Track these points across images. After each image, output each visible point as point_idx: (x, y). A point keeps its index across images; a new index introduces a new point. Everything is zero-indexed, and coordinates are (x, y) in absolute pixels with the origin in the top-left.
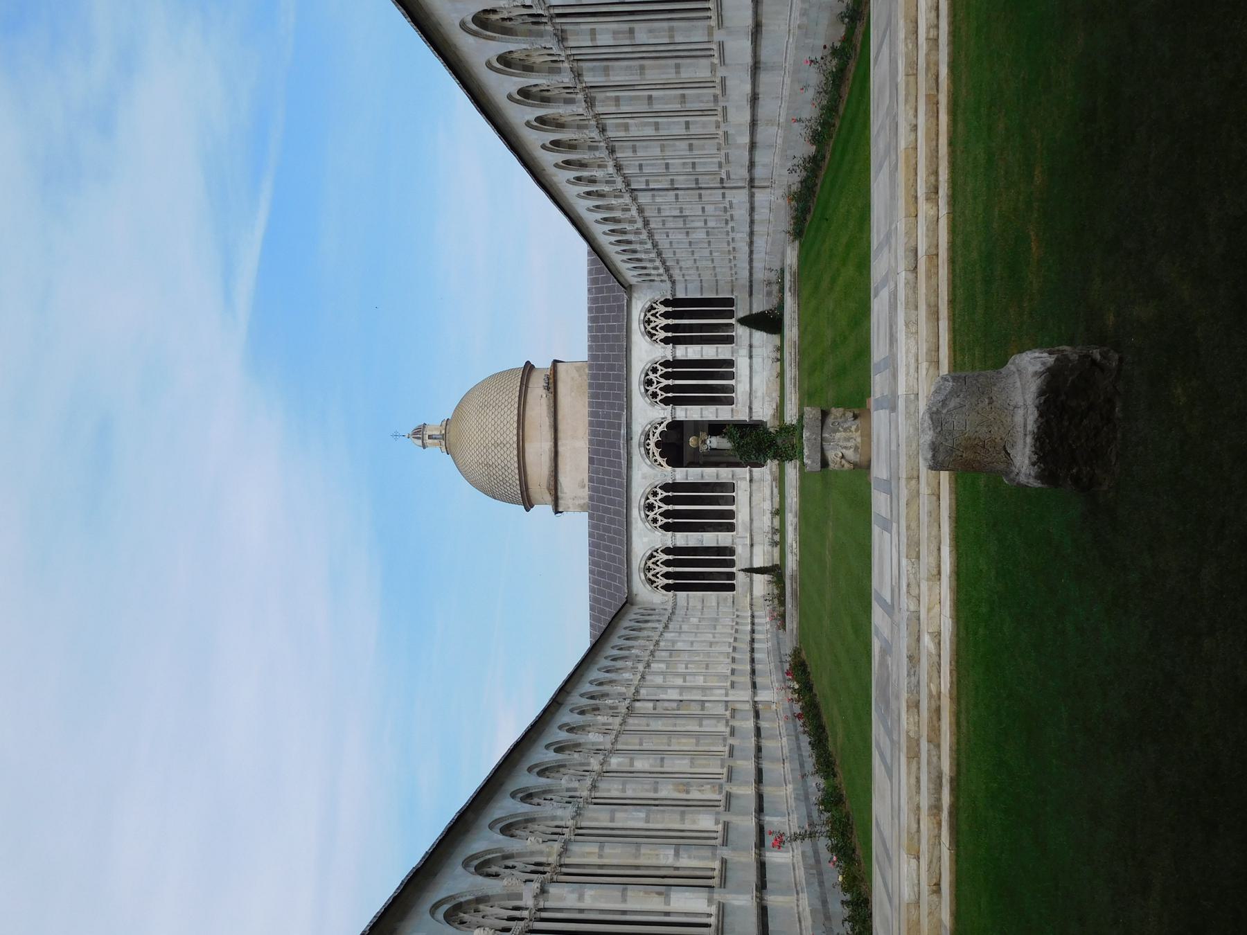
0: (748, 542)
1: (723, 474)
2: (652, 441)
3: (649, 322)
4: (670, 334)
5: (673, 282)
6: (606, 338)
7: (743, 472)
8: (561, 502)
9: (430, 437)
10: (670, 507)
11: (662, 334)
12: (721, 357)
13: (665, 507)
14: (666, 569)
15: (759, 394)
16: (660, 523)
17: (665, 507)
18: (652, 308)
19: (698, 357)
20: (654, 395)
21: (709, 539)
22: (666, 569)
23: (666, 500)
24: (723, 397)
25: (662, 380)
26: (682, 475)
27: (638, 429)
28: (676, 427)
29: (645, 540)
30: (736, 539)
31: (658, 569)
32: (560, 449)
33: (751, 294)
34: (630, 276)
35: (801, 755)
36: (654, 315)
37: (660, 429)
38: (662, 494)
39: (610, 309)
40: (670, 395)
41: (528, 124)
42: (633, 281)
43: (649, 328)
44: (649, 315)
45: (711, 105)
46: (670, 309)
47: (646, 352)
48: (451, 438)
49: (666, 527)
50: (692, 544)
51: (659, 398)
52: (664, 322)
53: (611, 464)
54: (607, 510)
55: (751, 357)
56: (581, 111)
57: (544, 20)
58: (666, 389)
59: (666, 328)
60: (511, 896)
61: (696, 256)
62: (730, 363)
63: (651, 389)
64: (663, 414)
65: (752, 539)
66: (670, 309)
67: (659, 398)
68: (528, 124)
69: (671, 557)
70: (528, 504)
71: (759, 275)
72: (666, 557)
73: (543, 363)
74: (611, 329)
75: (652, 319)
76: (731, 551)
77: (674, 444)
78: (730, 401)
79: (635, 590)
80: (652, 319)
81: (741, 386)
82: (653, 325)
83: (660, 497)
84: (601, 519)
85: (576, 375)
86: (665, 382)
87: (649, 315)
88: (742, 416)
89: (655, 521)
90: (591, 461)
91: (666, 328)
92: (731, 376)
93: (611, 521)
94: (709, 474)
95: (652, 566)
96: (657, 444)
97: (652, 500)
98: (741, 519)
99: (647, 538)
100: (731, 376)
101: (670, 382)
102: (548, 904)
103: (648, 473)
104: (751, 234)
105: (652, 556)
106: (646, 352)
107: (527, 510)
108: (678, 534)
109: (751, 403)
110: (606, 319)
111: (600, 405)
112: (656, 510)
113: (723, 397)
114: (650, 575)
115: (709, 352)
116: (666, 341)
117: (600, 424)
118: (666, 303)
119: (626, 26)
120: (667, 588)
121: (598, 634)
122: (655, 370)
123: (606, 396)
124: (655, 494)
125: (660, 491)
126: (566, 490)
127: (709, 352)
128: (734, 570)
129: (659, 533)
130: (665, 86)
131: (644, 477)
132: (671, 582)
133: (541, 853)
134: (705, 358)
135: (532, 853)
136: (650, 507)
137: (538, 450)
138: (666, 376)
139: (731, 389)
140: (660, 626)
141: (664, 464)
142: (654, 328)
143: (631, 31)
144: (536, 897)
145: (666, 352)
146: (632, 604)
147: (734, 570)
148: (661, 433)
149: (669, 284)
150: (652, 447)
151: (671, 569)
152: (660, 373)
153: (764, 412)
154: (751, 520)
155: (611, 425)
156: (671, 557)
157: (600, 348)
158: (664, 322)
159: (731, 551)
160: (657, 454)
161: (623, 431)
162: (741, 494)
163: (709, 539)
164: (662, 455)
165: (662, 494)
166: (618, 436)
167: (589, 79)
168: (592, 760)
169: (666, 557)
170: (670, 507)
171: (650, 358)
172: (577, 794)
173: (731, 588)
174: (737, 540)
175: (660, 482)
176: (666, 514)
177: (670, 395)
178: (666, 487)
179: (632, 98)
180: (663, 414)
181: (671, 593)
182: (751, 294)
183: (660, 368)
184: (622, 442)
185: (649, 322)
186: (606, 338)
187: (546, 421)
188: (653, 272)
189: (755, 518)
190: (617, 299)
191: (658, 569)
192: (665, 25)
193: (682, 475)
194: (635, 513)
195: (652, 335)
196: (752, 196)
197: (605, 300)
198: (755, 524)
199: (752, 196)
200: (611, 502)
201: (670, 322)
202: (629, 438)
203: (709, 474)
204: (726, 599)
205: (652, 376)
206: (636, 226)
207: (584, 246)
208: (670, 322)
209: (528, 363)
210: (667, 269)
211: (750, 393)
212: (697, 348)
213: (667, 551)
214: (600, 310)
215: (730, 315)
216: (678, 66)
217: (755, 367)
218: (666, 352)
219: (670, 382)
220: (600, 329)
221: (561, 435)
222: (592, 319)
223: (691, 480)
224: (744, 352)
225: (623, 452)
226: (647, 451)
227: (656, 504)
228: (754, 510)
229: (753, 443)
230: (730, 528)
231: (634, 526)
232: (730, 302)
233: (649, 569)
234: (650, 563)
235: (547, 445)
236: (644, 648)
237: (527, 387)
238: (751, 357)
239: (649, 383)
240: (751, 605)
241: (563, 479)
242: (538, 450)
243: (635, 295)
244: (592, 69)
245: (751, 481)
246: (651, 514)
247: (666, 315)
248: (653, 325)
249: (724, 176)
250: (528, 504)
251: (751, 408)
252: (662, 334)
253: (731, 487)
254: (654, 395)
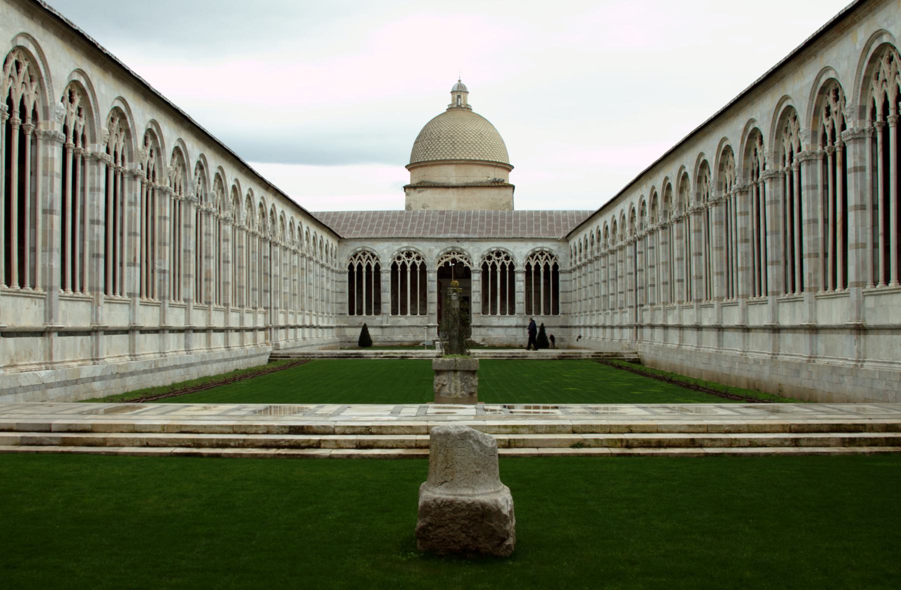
0: (384, 324)
1: (433, 308)
2: (457, 257)
3: (542, 254)
4: (533, 269)
5: (570, 272)
6: (530, 223)
7: (434, 322)
8: (412, 191)
9: (459, 97)
10: (409, 269)
11: (533, 264)
12: (517, 306)
13: (409, 266)
14: (364, 266)
15: (490, 333)
16: (397, 262)
17: (409, 266)
18: (552, 256)
19: (517, 289)
20: (489, 258)
21: (386, 297)
22: (364, 266)
23: (414, 266)
24: (488, 306)
25: (500, 263)
26: (432, 277)
27: (465, 246)
28: (465, 273)
29: (385, 251)
30: (386, 317)
31: (364, 260)
32: (450, 191)
33: (562, 327)
34: (575, 241)
35: (233, 359)
36: (547, 258)
37: (465, 262)
38: (418, 263)
39: (551, 227)
40: (490, 269)
41: (683, 167)
42: (571, 243)
43: (537, 254)
44: (547, 254)
45: (694, 297)
46: (551, 269)
47: (520, 253)
48: (459, 114)
49: (394, 266)
50: (383, 284)
51: (488, 262)
52: (542, 265)
53: (440, 227)
54: (406, 224)
55: (517, 327)
56: (692, 205)
57: (755, 179)
58: (494, 266)
59: (537, 267)
60: (130, 153)
61: (589, 288)
62: (512, 312)
63: (494, 256)
64: (476, 264)
65: (386, 327)
66: (551, 269)
67: (488, 262)
68: (683, 167)
69: (373, 269)
70: (410, 167)
71: (575, 333)
72: (373, 266)
73: (512, 178)
74: (537, 227)
75: (544, 257)
76: (378, 312)
77: (454, 272)
78: (485, 311)
79: (349, 243)
80: (544, 257)
81: (495, 320)
82: (540, 257)
83: (416, 261)
84: (400, 220)
85: (504, 202)
86: (499, 265)
87: (547, 254)
88: (475, 320)
89: (399, 258)
90: (442, 213)
91: (537, 267)
92: (503, 312)
93: (399, 227)
94: (433, 297)
95: (366, 256)
96: (454, 261)
97: (414, 256)
98: (401, 320)
99: (386, 254)
100: (503, 312)
101: (499, 269)
102: (126, 181)
103: (432, 254)
104: (604, 327)
105: (373, 256)
106: (520, 253)
107: (406, 167)
108: (389, 275)
109: (484, 327)
110: (544, 224)
111: (482, 219)
112: (407, 259)
113: (488, 306)
114: (360, 254)
115: (520, 297)
116: (528, 266)
117: (468, 219)
118: (556, 266)
119: (750, 237)
120: (351, 267)
121: (318, 218)
122: (507, 258)
123: (489, 223)
124: (418, 258)
125: (420, 261)
126: (420, 195)
127: (520, 297)
128: (364, 315)
129: (390, 261)
130: (708, 265)
131: (430, 251)
132: (355, 269)
133: (161, 176)
134: (516, 294)
135: (161, 169)
136: (409, 255)
137: (451, 175)
138: (503, 266)
139: (494, 313)
140: (324, 262)
141: (440, 265)
142: (537, 258)
143: (746, 241)
144: (131, 172)
145: (520, 266)
146: (339, 242)
147: (364, 315)
148: (462, 263)
149: (569, 268)
150: (452, 256)
151: (364, 269)
153: (476, 336)
154: (400, 327)
155: (468, 227)
156: (373, 269)
157: (524, 219)
158: (542, 265)
159: (378, 312)
160: (447, 260)
161: (463, 236)
162: (418, 320)
163: (386, 297)
164: (447, 263)
165: (418, 263)
166: (460, 232)
167: (713, 211)
168: (227, 212)
169: (373, 266)
170: (409, 269)
171: (516, 255)
172: (204, 202)
173: (351, 312)
174: (385, 317)
175: (428, 261)
176: (404, 266)
177: (490, 269)
178: (423, 266)
179: (700, 241)
180: (476, 264)
181: (347, 270)
182: (562, 327)
184: (456, 235)
185: (542, 254)
186: (530, 223)
187: (471, 180)
188: (578, 257)
189: (402, 330)
190: (559, 231)
191: (364, 260)
192: (751, 265)
193: (432, 277)
194: (405, 244)
195: (532, 256)
196: (631, 327)
197: (558, 224)
198: (397, 330)
199: (631, 327)
200: (412, 227)
201: (542, 269)
202: (458, 240)
203: (433, 297)
204: (343, 308)
205: (503, 256)
206: (610, 245)
207: (596, 208)
208: (542, 269)
209: (513, 167)
210: (579, 267)
211: (490, 326)
212: (523, 289)
213: (378, 267)
214: (551, 219)
215: (547, 313)
216: (722, 273)
217: (510, 330)
218: (520, 266)
219: (499, 269)
220: (537, 219)
221: (461, 191)
222: (544, 214)
223: (429, 284)
224: (520, 322)
225: (449, 235)
226: (449, 253)
227: (411, 259)
228: (407, 329)
229: (456, 329)
230: (394, 312)
231: (395, 243)
232: (556, 311)
233: (364, 254)
234: (368, 254)
235: (453, 181)
236: (308, 250)
237: (496, 166)
238: (517, 327)
239: (498, 254)
240: (340, 327)
241: (428, 194)
242: (451, 175)
243: (561, 244)
244: (720, 213)
245: (428, 327)
246: (403, 256)
247: (547, 267)
248: (540, 257)
249: (645, 307)
250: (410, 167)
251: (480, 326)
252: (533, 264)
253: (424, 312)
254: (489, 258)
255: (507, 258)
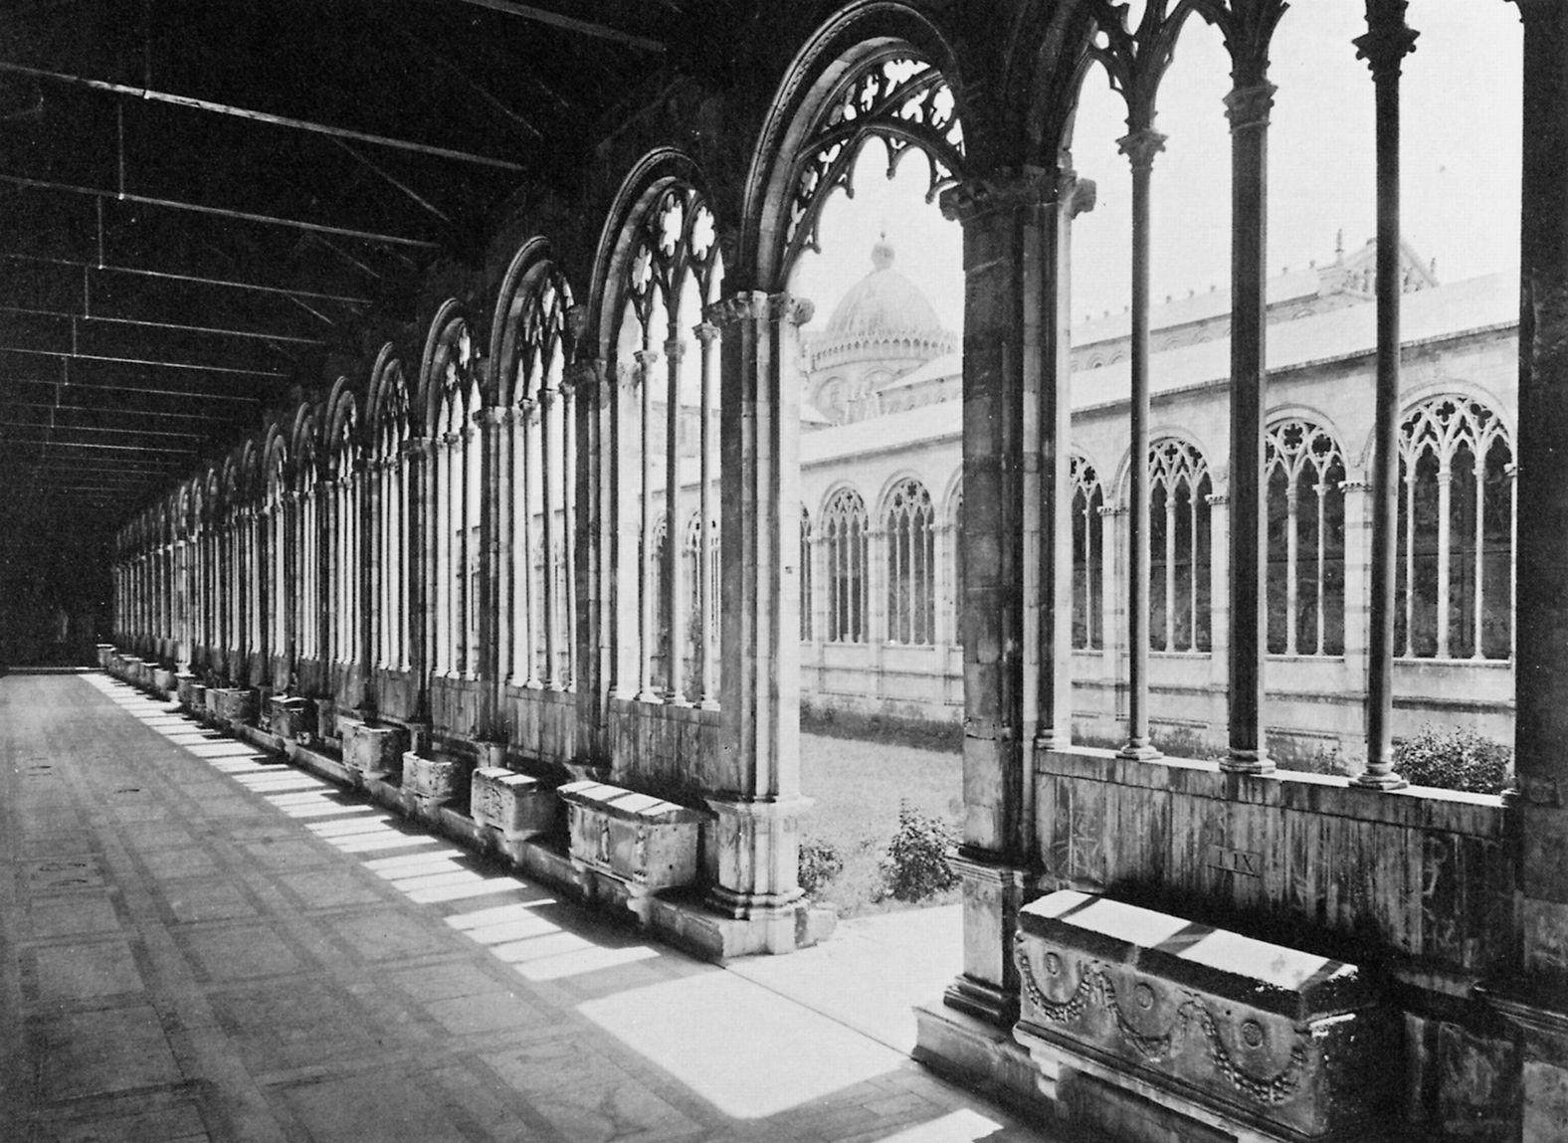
25: (1299, 466)
36: (1463, 425)
46: (1479, 470)
66: (1479, 470)
80: (1454, 421)
82: (1436, 423)
86: (1293, 476)
122: (1322, 445)
142: (1428, 429)
152: (1315, 459)
158: (1445, 455)
183: (1328, 457)
205: (1308, 439)
255: (1322, 445)
